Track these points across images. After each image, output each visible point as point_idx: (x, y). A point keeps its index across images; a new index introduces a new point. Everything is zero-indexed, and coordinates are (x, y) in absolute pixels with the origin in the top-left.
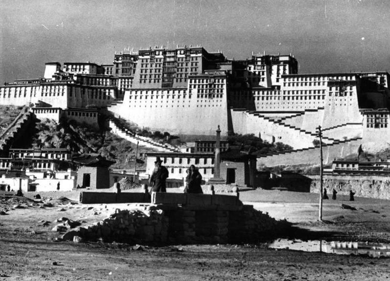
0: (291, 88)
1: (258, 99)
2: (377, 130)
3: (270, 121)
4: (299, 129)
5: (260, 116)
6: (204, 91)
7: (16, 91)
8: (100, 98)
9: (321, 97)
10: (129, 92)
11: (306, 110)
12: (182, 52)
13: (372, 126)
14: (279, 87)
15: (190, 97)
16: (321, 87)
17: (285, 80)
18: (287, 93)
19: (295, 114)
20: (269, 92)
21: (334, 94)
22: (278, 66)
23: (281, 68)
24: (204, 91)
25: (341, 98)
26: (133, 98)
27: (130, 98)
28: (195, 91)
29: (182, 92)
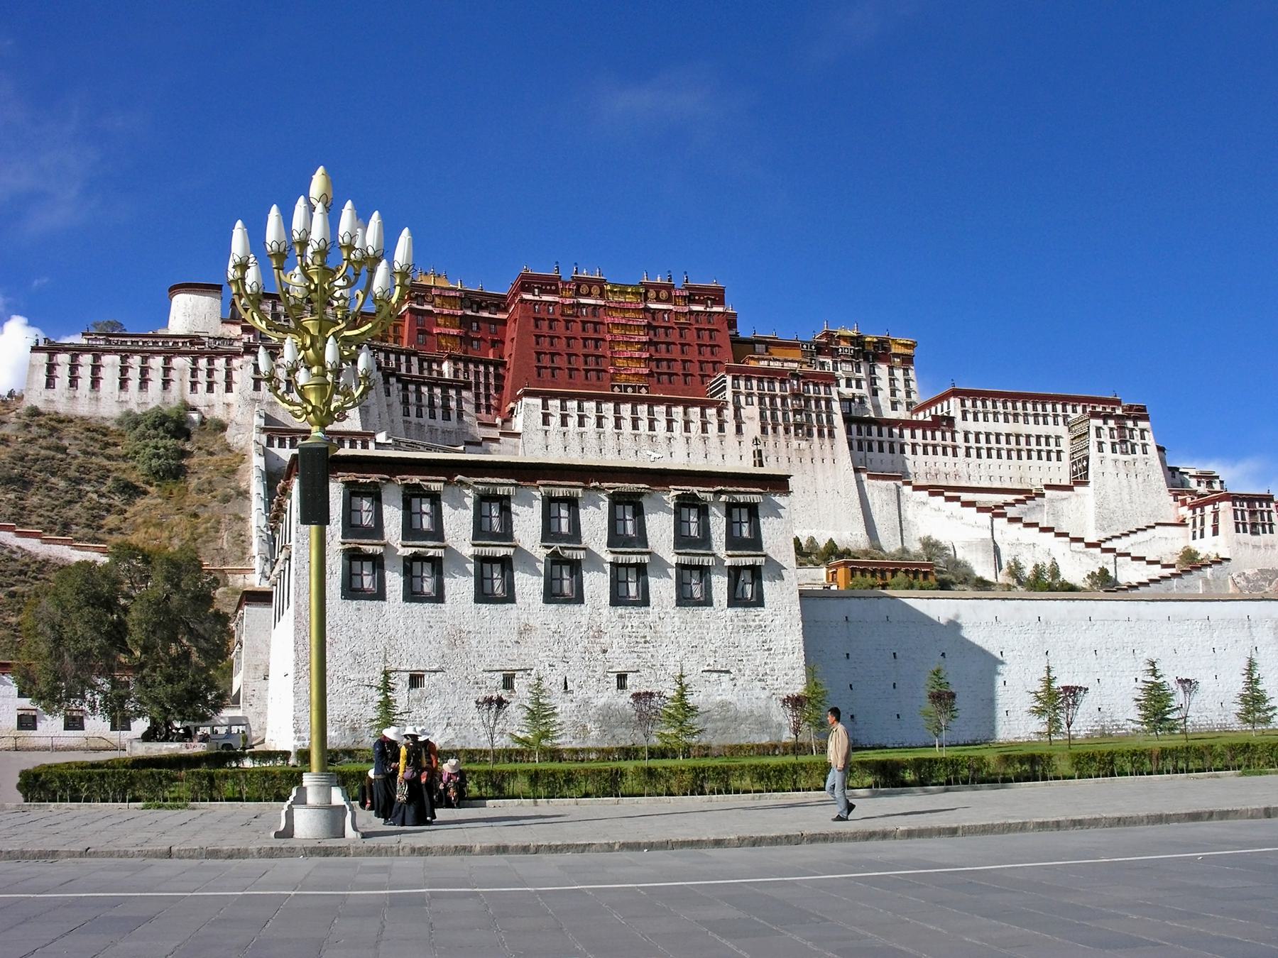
0: (981, 426)
1: (914, 452)
2: (1256, 538)
3: (980, 510)
4: (1066, 535)
5: (948, 499)
6: (780, 414)
7: (124, 370)
8: (433, 416)
9: (1054, 456)
10: (539, 401)
11: (1048, 487)
12: (664, 294)
13: (1245, 531)
14: (950, 421)
15: (739, 430)
16: (1050, 429)
17: (963, 405)
18: (972, 437)
19: (1021, 497)
20: (929, 433)
21: (1107, 447)
22: (891, 368)
23: (899, 373)
24: (780, 414)
25: (1125, 457)
26: (555, 421)
27: (546, 421)
28: (751, 412)
29: (711, 412)
